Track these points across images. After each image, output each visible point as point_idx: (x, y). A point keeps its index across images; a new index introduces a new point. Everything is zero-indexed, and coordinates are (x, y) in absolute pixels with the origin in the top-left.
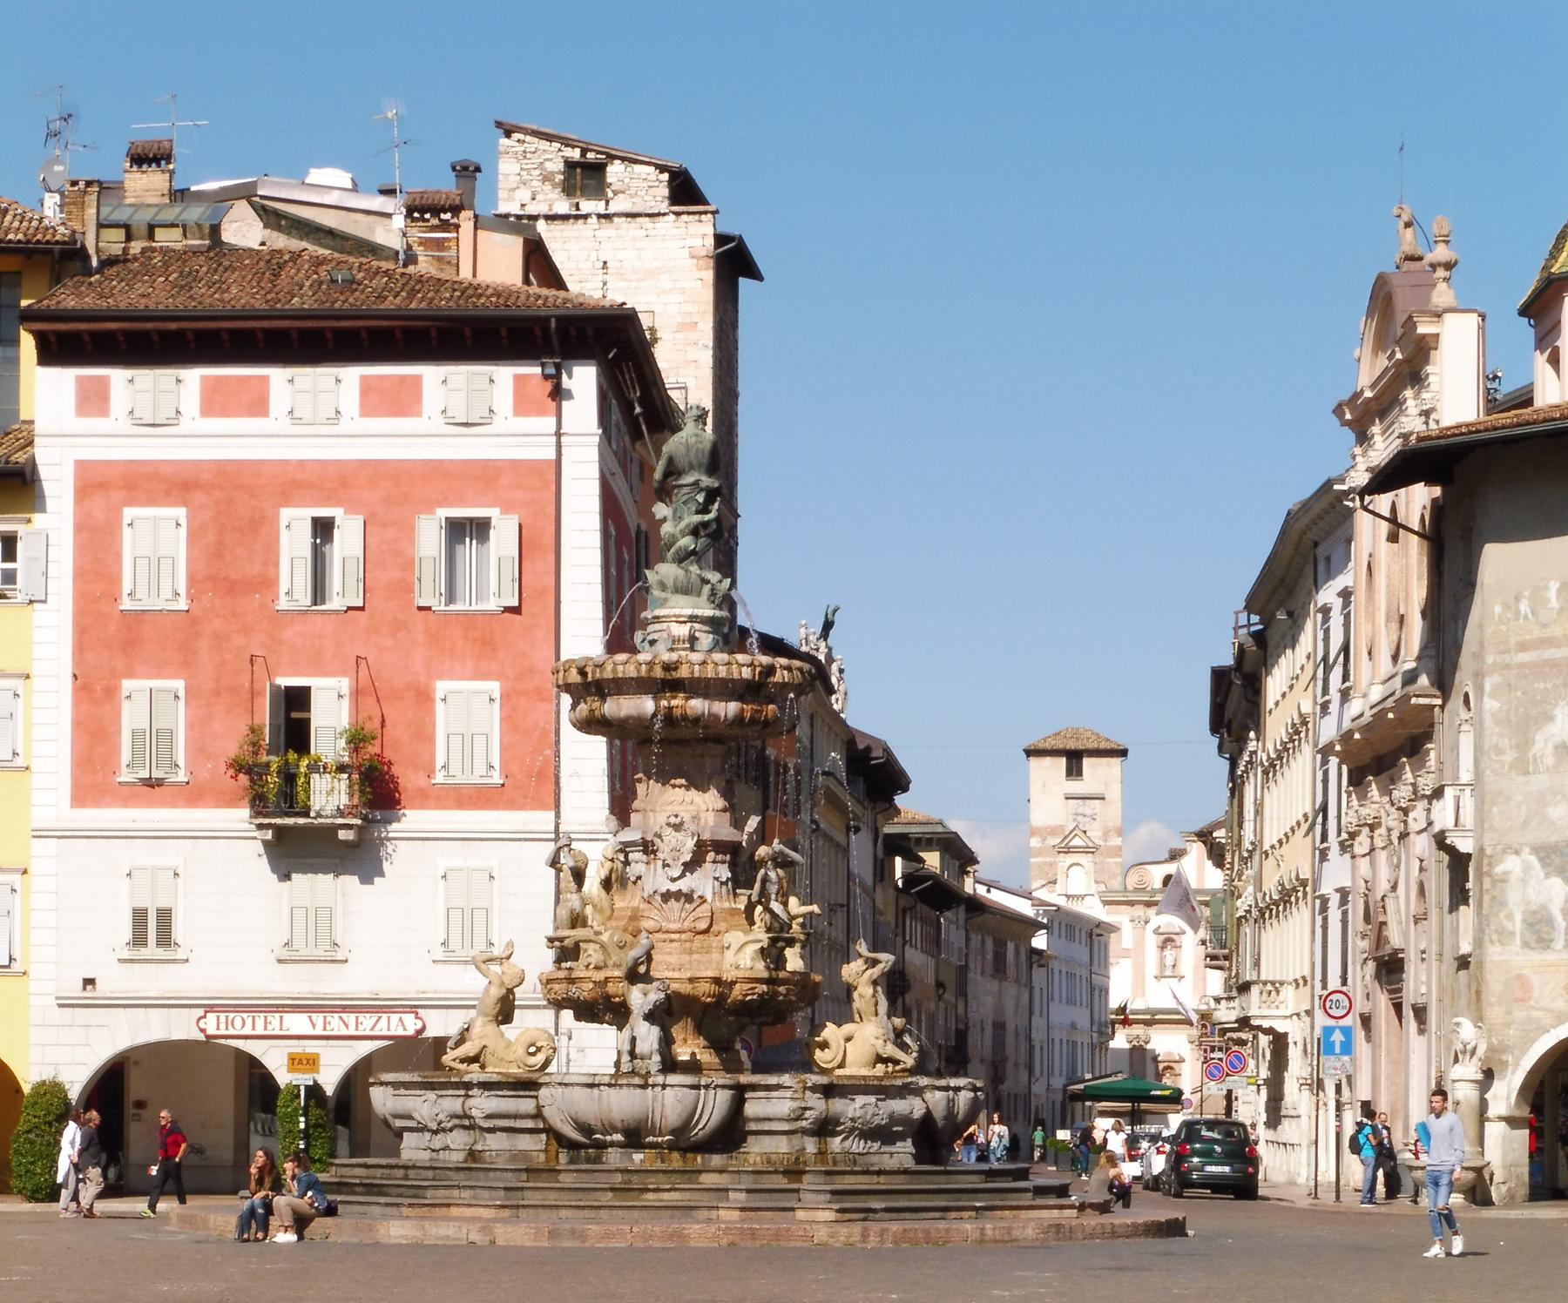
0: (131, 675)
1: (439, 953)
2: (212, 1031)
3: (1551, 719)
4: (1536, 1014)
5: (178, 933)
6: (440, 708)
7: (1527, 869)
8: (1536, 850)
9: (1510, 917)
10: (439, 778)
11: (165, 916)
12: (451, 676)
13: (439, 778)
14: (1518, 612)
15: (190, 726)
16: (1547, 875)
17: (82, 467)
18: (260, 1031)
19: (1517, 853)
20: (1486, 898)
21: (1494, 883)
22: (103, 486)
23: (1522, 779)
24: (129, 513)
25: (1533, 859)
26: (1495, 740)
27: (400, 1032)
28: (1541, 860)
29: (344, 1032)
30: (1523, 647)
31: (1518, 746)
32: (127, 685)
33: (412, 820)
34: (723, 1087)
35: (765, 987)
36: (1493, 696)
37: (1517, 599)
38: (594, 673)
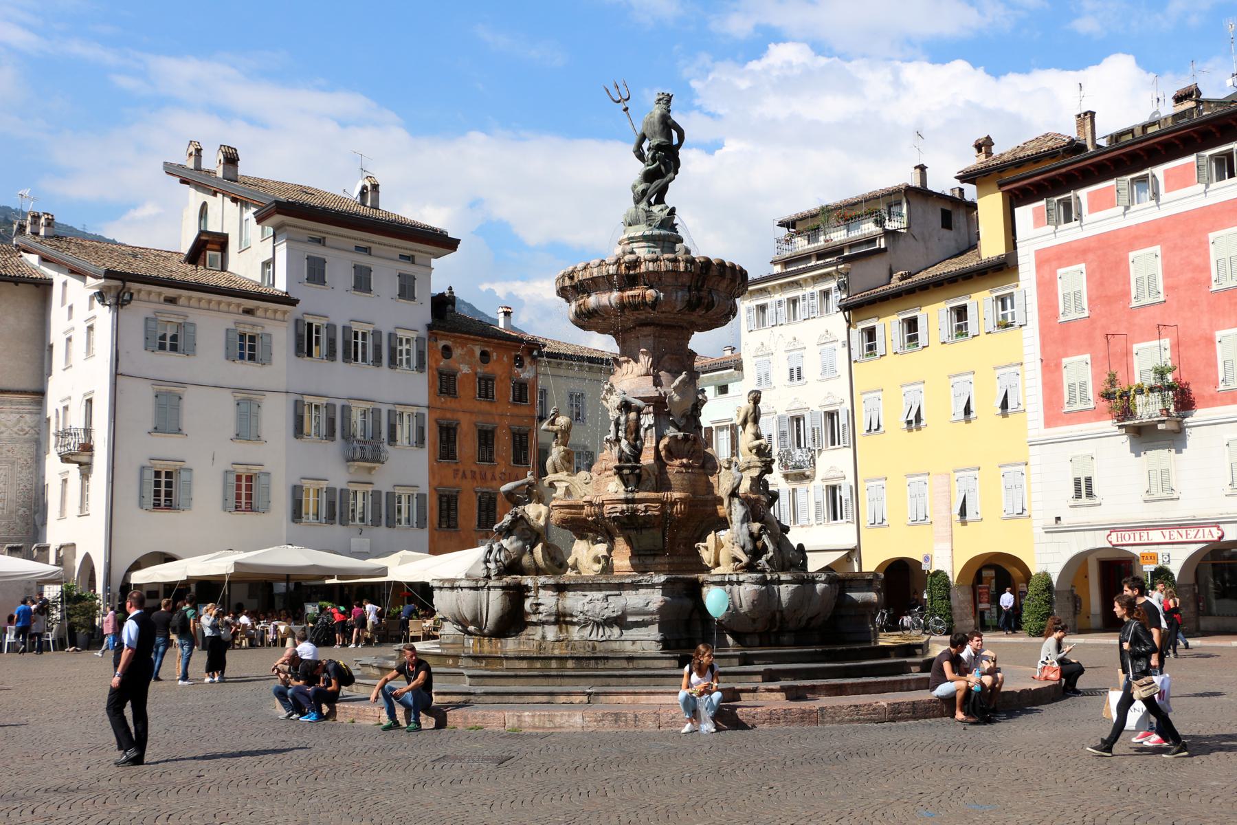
0: (1066, 356)
1: (1229, 490)
2: (1115, 542)
5: (1095, 491)
6: (1218, 345)
10: (1221, 387)
11: (1089, 481)
12: (1224, 328)
13: (1221, 387)
15: (1094, 378)
17: (1038, 252)
18: (1138, 541)
22: (1048, 261)
24: (1060, 272)
27: (1210, 538)
29: (1180, 540)
32: (1065, 361)
33: (1199, 415)
34: (495, 587)
35: (624, 506)
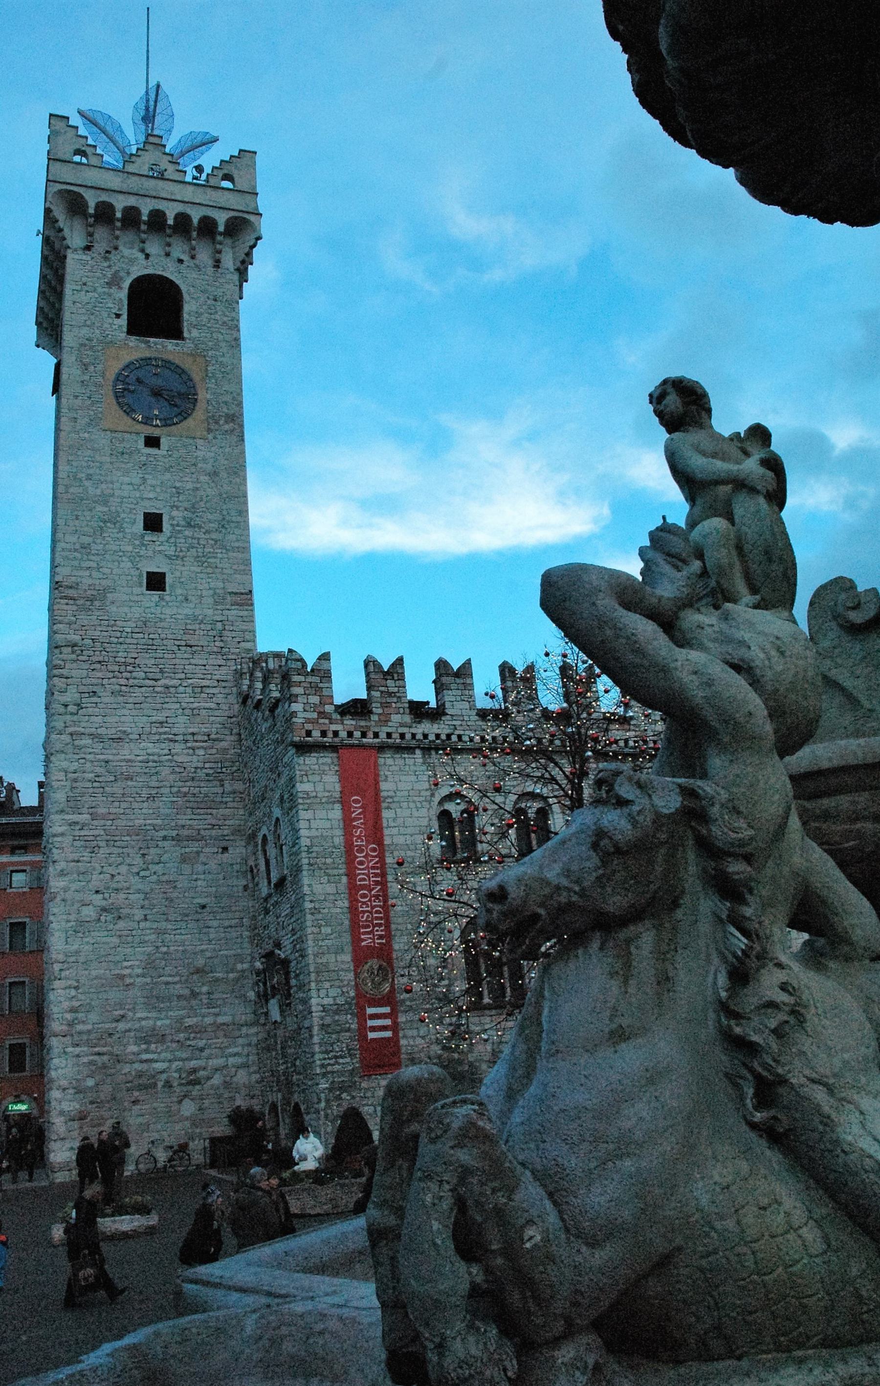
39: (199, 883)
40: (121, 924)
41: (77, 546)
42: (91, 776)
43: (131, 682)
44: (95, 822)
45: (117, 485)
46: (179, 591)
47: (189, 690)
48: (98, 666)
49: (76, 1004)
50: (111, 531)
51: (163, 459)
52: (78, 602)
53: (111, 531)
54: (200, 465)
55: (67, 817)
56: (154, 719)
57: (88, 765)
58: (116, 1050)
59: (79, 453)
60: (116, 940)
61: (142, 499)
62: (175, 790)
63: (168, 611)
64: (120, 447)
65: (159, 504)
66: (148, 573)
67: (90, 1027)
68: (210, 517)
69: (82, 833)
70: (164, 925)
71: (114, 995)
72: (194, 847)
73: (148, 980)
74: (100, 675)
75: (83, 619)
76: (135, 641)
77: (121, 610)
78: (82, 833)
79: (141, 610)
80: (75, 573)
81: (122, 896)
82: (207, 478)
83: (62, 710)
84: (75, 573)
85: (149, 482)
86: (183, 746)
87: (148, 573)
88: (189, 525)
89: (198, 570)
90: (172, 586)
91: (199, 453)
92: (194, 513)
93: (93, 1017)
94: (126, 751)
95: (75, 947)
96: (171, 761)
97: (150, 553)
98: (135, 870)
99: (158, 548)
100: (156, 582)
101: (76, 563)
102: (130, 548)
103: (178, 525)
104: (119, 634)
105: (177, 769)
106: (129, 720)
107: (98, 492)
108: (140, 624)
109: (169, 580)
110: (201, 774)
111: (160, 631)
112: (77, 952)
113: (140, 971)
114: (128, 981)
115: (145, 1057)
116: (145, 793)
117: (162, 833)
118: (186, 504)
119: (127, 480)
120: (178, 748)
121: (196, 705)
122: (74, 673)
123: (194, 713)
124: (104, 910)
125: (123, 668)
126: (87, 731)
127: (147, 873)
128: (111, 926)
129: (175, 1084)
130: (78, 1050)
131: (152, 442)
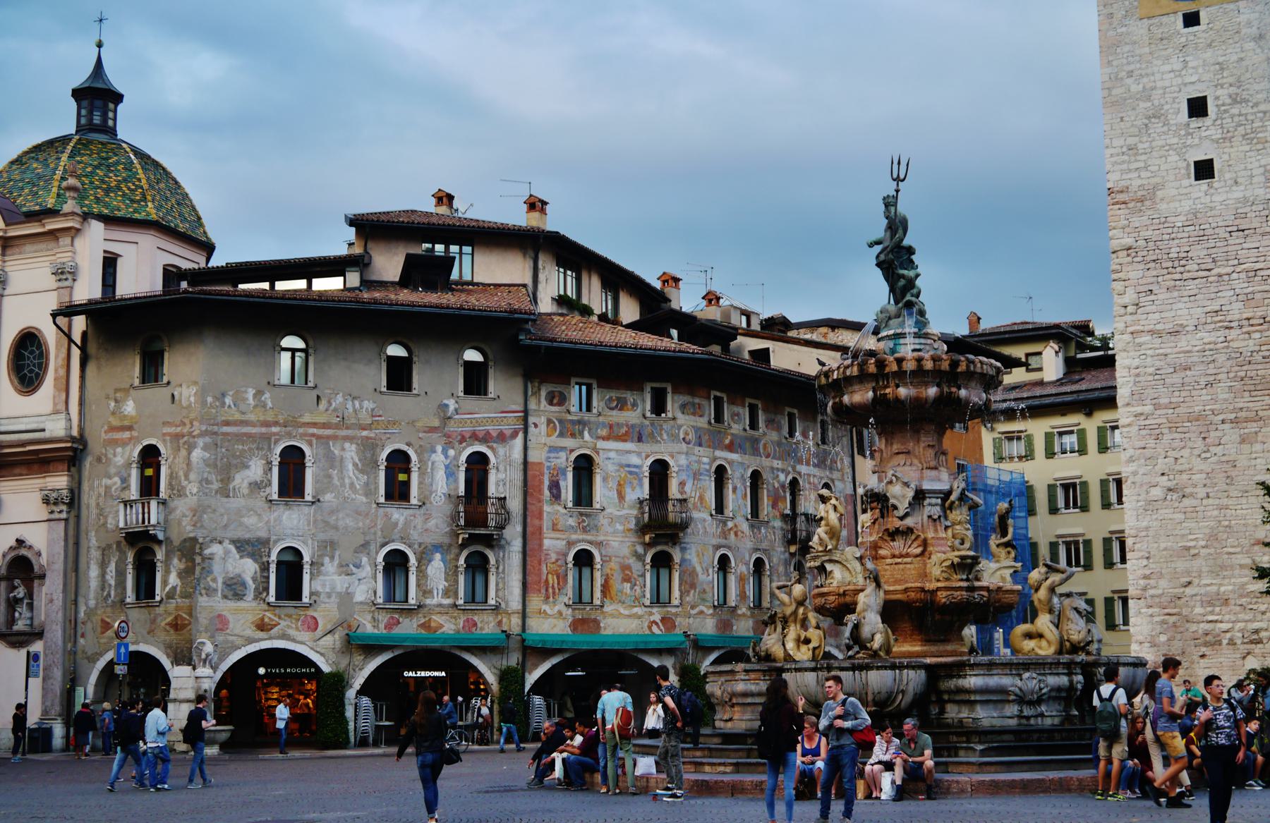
3: (248, 467)
4: (231, 638)
7: (227, 552)
8: (233, 542)
9: (214, 580)
14: (224, 403)
16: (241, 557)
19: (220, 543)
20: (198, 569)
21: (203, 559)
23: (225, 500)
25: (232, 548)
26: (205, 475)
28: (237, 548)
30: (227, 423)
31: (222, 480)
36: (205, 448)
37: (223, 395)
38: (968, 366)
39: (1258, 461)
40: (1186, 502)
41: (1124, 149)
42: (1151, 370)
43: (1186, 276)
44: (1158, 412)
45: (1158, 76)
46: (1228, 176)
47: (1243, 275)
48: (1152, 265)
49: (1148, 572)
50: (1157, 127)
51: (1204, 35)
52: (1130, 205)
53: (1157, 127)
54: (1244, 31)
55: (1132, 409)
56: (1208, 309)
57: (1149, 359)
58: (1185, 612)
59: (1119, 50)
60: (1182, 516)
61: (1185, 85)
62: (1231, 375)
63: (1217, 198)
64: (1158, 32)
65: (1200, 86)
66: (1196, 163)
67: (1160, 592)
68: (1257, 87)
69: (1147, 422)
70: (1225, 501)
71: (1181, 565)
72: (1252, 427)
73: (1212, 551)
74: (1155, 273)
75: (1136, 221)
76: (1186, 235)
77: (1172, 205)
78: (1147, 422)
79: (1191, 202)
80: (1125, 176)
81: (1185, 476)
82: (1252, 44)
83: (1122, 311)
84: (1125, 176)
85: (1190, 64)
86: (1239, 332)
87: (1196, 163)
88: (1235, 100)
89: (1247, 148)
90: (1220, 171)
91: (1243, 18)
92: (1239, 87)
93: (1163, 583)
94: (1183, 343)
95: (1145, 524)
96: (1227, 347)
97: (1196, 141)
98: (1196, 452)
99: (1204, 134)
100: (1204, 170)
101: (1125, 166)
102: (1175, 140)
103: (1223, 105)
104: (1170, 230)
105: (1233, 355)
106: (1185, 313)
107: (1141, 86)
108: (1190, 216)
109: (1217, 166)
110: (1258, 357)
111: (1210, 220)
112: (1147, 528)
113: (1203, 543)
114: (1193, 552)
115: (1211, 618)
116: (1203, 382)
117: (1221, 417)
118: (1231, 80)
119: (1167, 68)
120: (1233, 334)
121: (1250, 290)
122: (1132, 275)
123: (1248, 299)
124: (1170, 490)
125: (1176, 264)
126: (1146, 328)
127: (1208, 455)
128: (1177, 504)
129: (1239, 642)
130: (1150, 611)
131: (1191, 20)
